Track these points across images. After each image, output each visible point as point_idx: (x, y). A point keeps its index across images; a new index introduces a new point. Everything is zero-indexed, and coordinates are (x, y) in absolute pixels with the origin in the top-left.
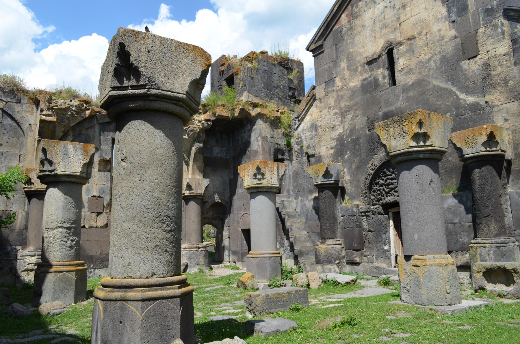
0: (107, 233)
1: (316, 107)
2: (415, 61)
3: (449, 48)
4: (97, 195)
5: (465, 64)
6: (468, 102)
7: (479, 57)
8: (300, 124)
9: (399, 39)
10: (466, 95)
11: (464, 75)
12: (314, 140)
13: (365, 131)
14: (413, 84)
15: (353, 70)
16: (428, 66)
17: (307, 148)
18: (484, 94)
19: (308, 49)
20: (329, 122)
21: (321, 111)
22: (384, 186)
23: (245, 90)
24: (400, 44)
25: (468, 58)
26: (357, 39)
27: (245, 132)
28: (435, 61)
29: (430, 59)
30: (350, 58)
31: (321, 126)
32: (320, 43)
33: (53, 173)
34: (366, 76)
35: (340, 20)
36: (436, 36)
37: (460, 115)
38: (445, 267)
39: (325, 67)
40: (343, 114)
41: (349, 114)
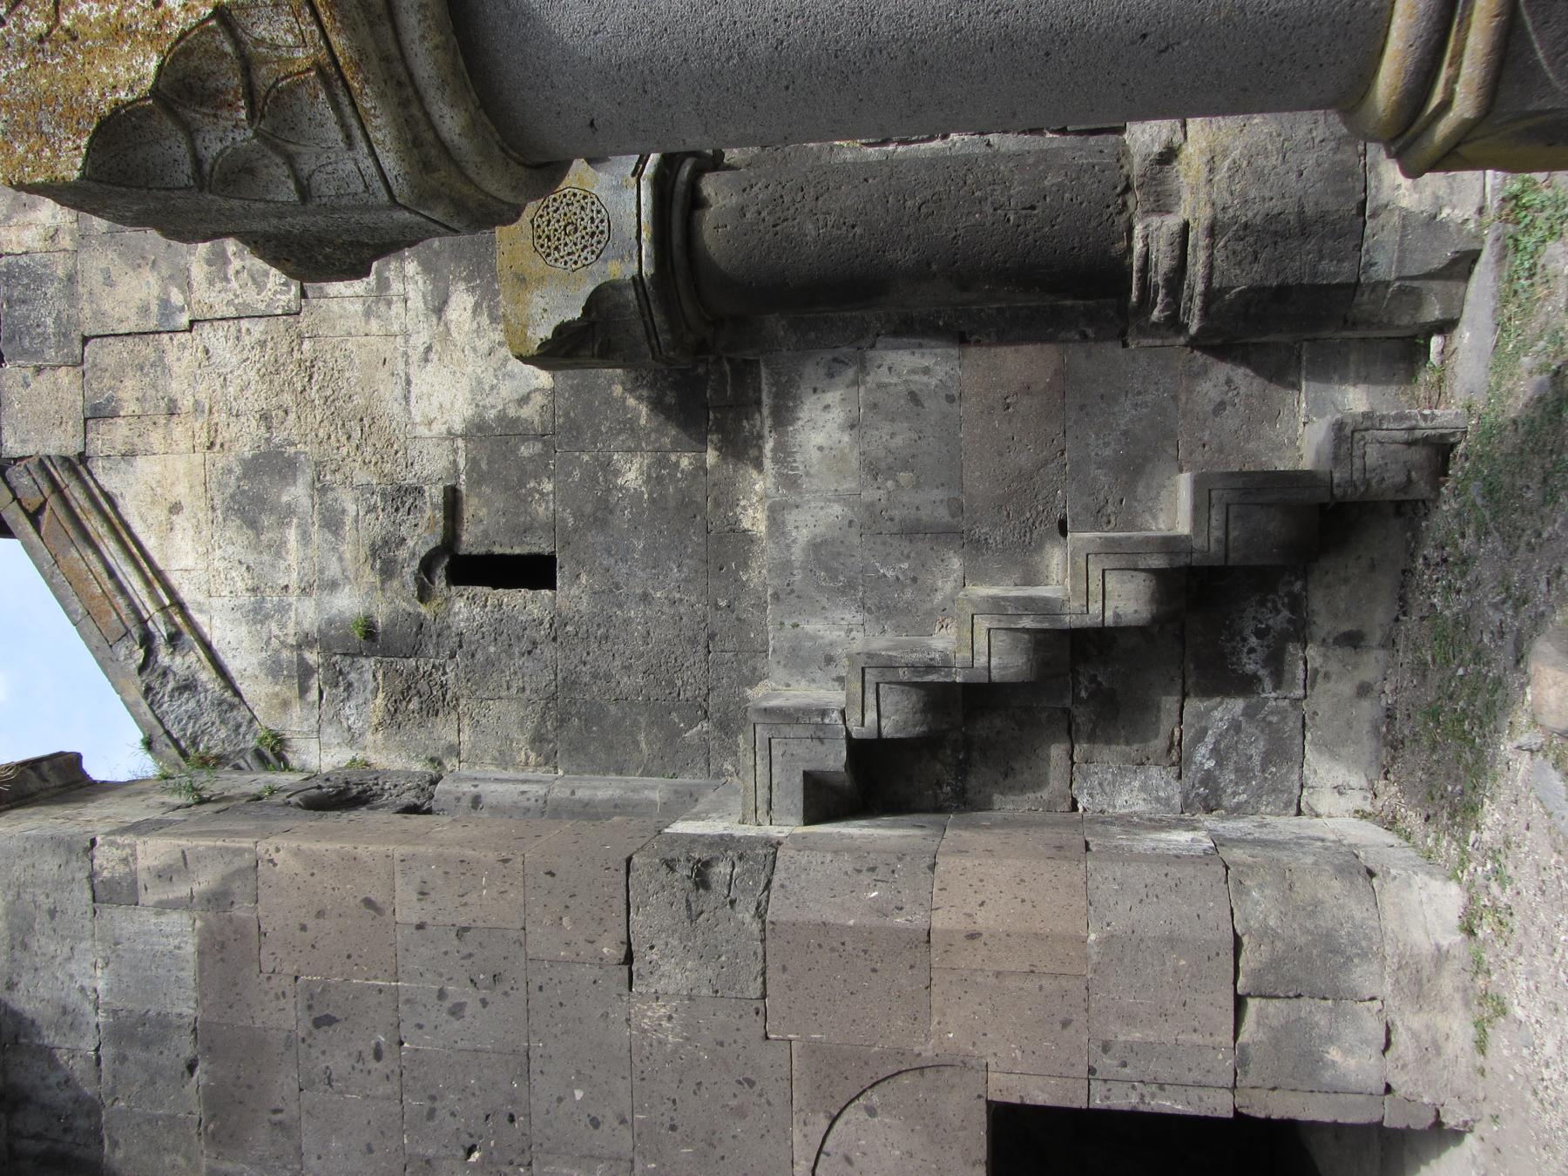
1: (129, 455)
8: (207, 647)
12: (350, 505)
17: (388, 571)
31: (265, 417)
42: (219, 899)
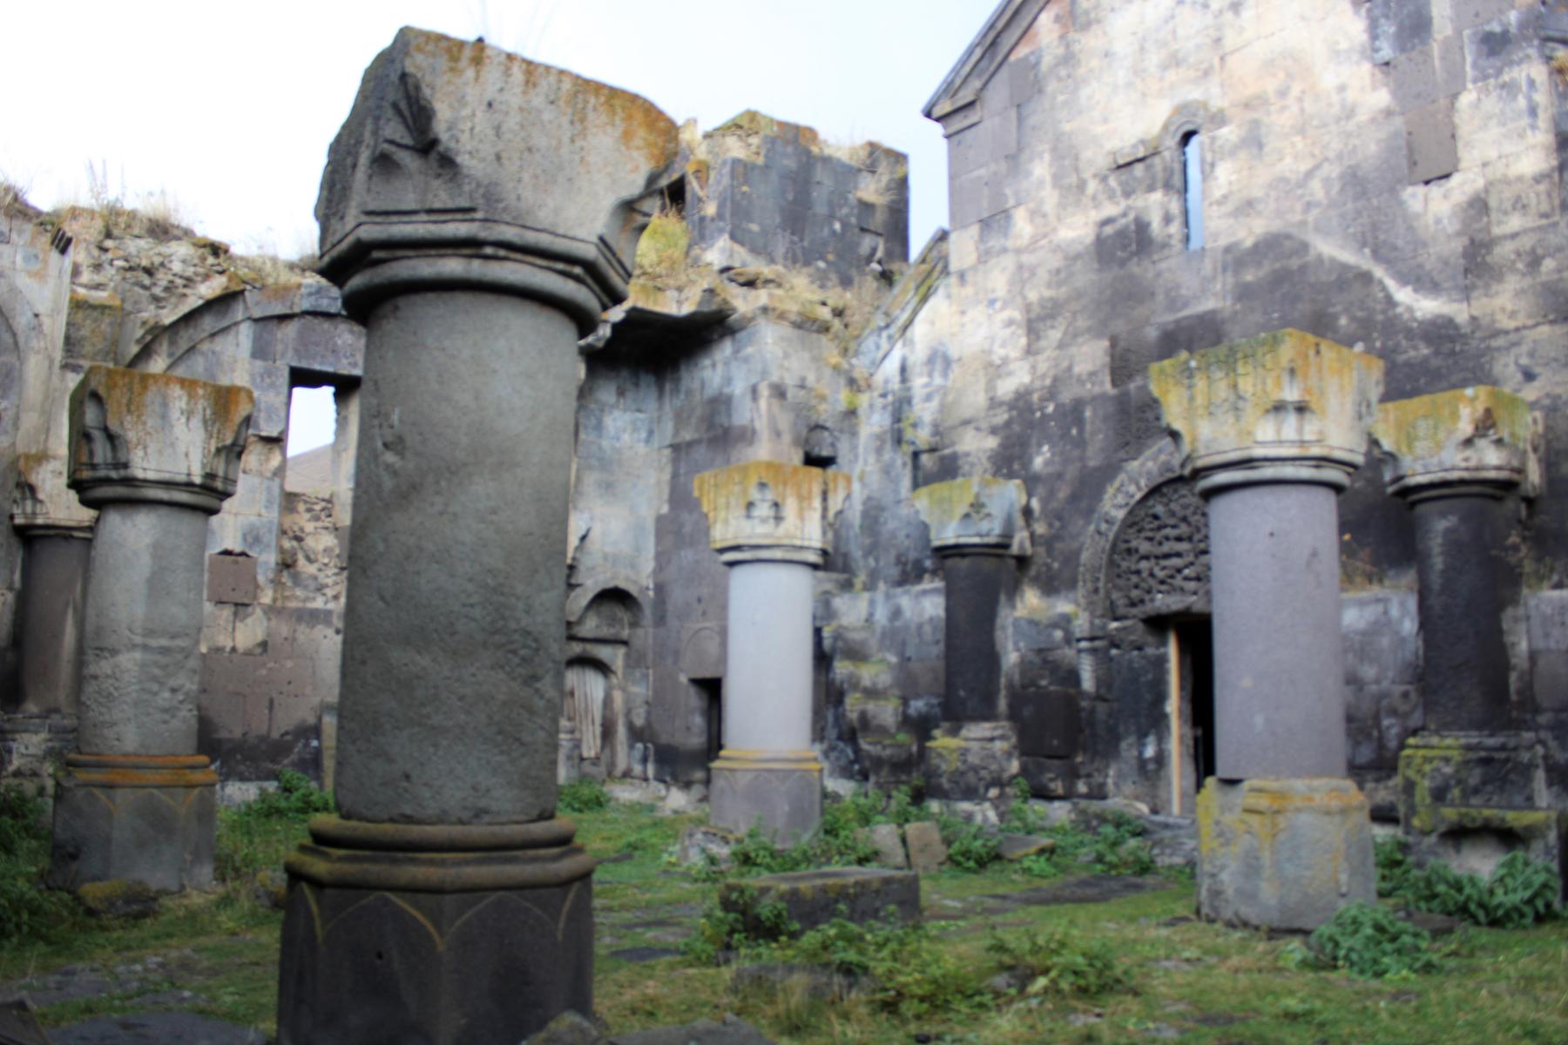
0: (264, 672)
1: (949, 296)
2: (1264, 175)
3: (1370, 147)
4: (238, 549)
5: (1414, 196)
6: (1419, 314)
7: (1456, 179)
9: (1217, 103)
10: (1416, 291)
11: (1410, 228)
13: (1102, 383)
14: (1256, 246)
15: (1073, 191)
16: (1302, 196)
18: (1466, 293)
19: (928, 115)
20: (986, 347)
21: (963, 313)
22: (1153, 561)
23: (721, 231)
24: (1219, 119)
25: (1427, 178)
26: (1084, 92)
27: (714, 366)
28: (1326, 181)
29: (1309, 174)
30: (1065, 154)
32: (965, 96)
33: (122, 473)
34: (1110, 210)
35: (1031, 32)
36: (1330, 105)
37: (1394, 351)
38: (1337, 819)
39: (982, 172)
40: (1033, 328)
41: (1053, 327)
42: (754, 432)
